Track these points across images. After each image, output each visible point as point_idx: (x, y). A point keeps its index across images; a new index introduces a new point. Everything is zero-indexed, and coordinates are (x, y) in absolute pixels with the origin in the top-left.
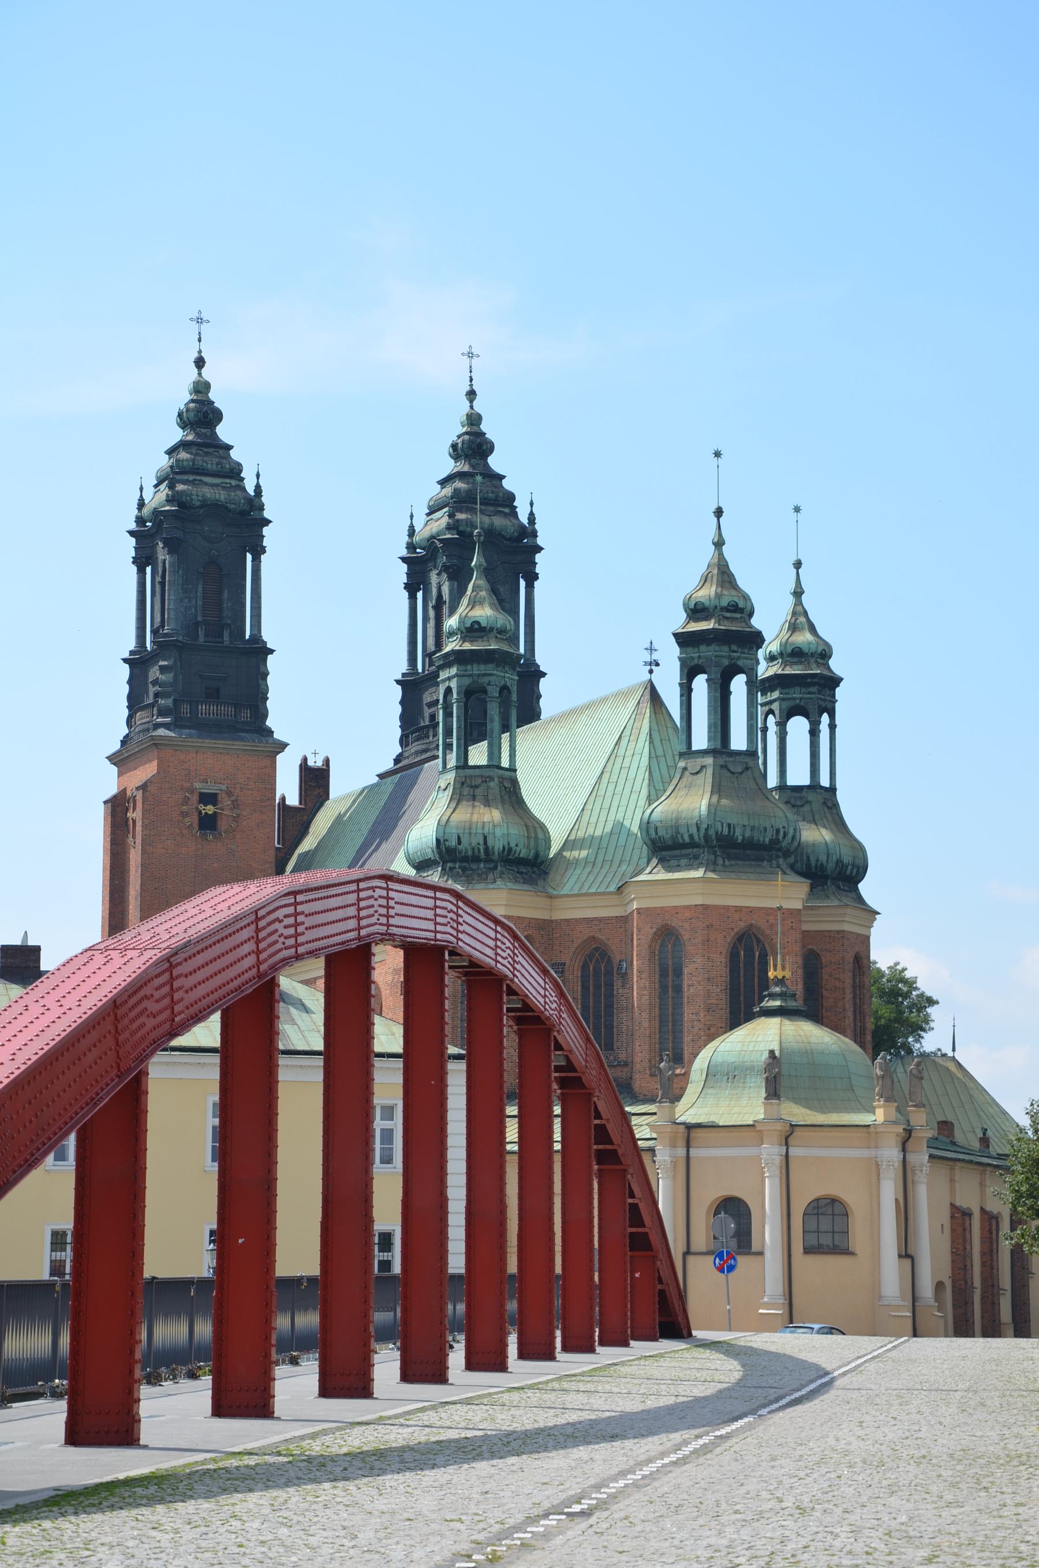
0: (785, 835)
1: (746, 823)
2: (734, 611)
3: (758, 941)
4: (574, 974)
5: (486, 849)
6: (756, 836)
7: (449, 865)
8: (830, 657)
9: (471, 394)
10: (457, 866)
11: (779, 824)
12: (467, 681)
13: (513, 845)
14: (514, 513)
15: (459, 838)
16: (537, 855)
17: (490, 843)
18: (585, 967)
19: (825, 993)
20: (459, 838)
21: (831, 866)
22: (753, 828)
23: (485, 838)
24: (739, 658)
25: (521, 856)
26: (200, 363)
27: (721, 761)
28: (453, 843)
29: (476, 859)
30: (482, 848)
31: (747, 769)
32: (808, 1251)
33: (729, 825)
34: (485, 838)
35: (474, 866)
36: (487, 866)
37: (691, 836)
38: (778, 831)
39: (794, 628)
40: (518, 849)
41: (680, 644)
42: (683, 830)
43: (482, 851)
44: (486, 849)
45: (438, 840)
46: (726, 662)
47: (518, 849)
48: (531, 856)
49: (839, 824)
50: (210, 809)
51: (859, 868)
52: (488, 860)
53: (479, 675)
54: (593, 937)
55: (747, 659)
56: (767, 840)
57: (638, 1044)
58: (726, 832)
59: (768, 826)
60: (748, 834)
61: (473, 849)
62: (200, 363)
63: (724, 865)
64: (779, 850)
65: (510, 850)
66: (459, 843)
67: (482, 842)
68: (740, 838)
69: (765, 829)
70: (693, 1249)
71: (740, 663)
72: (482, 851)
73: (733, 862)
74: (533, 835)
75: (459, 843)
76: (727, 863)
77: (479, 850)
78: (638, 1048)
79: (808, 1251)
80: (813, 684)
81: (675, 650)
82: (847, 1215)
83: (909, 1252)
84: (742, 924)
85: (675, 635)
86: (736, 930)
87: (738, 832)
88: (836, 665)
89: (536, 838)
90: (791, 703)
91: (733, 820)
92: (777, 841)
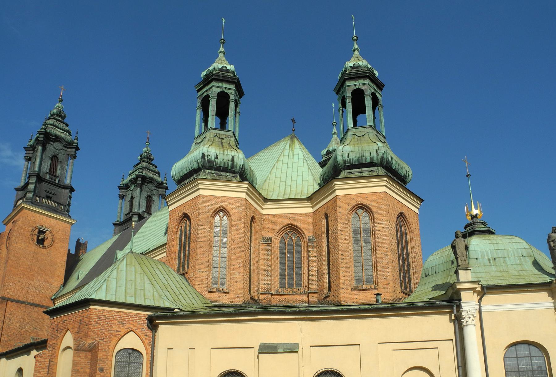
4: (276, 245)
5: (233, 164)
7: (208, 171)
10: (213, 172)
15: (217, 155)
17: (236, 160)
18: (282, 242)
20: (217, 155)
23: (233, 158)
29: (225, 170)
30: (230, 163)
34: (233, 158)
35: (223, 174)
36: (231, 175)
43: (230, 165)
44: (233, 164)
45: (204, 155)
50: (42, 236)
54: (290, 224)
57: (341, 272)
61: (225, 163)
66: (217, 158)
67: (230, 159)
72: (230, 165)
75: (217, 158)
77: (228, 164)
78: (341, 274)
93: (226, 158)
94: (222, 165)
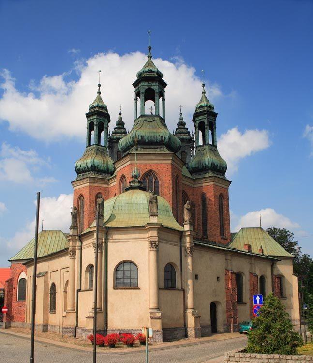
0: (165, 139)
1: (149, 135)
2: (150, 72)
3: (155, 176)
5: (87, 167)
6: (153, 139)
8: (213, 108)
9: (181, 114)
11: (162, 135)
12: (90, 122)
13: (96, 165)
14: (189, 135)
16: (108, 169)
19: (208, 206)
21: (210, 165)
22: (152, 137)
24: (151, 86)
25: (101, 169)
26: (120, 114)
27: (144, 118)
28: (79, 167)
31: (154, 120)
32: (115, 288)
33: (142, 136)
37: (130, 142)
38: (162, 137)
39: (201, 101)
40: (99, 167)
41: (135, 87)
42: (127, 141)
44: (87, 167)
45: (75, 167)
46: (147, 87)
47: (99, 167)
48: (106, 169)
49: (217, 155)
51: (223, 168)
52: (89, 171)
53: (92, 119)
55: (155, 86)
56: (158, 141)
58: (140, 138)
59: (158, 135)
60: (150, 138)
62: (120, 114)
63: (141, 150)
64: (164, 144)
65: (95, 167)
68: (147, 140)
69: (157, 136)
70: (83, 289)
71: (152, 87)
73: (145, 149)
74: (106, 163)
76: (142, 149)
79: (115, 288)
80: (205, 114)
81: (134, 89)
82: (138, 270)
83: (183, 288)
84: (147, 170)
85: (133, 84)
86: (144, 172)
87: (146, 138)
88: (215, 111)
89: (107, 164)
90: (199, 121)
91: (143, 134)
92: (162, 141)
93: (84, 165)
94: (84, 170)
